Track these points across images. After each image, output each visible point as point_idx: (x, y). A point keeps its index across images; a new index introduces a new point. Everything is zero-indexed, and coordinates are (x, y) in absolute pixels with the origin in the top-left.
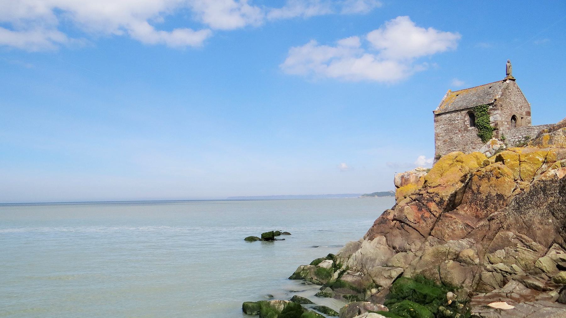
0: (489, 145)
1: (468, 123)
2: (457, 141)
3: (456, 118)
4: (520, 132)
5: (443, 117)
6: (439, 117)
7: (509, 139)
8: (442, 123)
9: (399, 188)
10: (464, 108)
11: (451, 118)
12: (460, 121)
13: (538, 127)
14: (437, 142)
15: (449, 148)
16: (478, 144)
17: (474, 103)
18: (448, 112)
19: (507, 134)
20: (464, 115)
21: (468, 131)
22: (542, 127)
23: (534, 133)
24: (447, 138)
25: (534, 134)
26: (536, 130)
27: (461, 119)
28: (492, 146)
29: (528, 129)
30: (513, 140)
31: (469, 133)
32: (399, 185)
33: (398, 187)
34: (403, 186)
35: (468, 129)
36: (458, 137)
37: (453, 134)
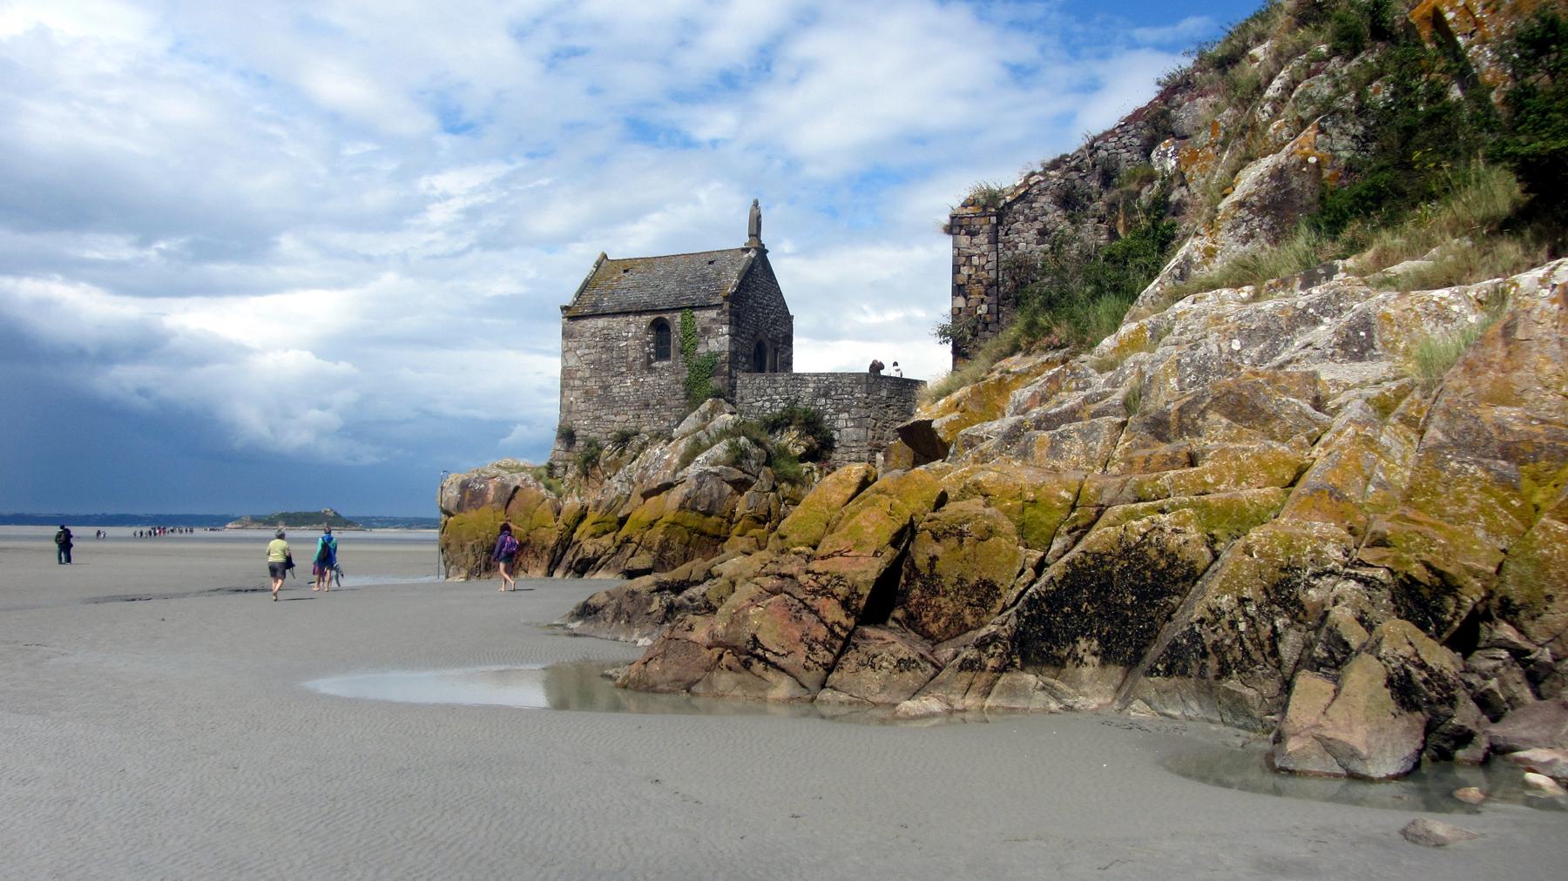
0: (705, 413)
7: (751, 400)
8: (586, 340)
9: (453, 516)
10: (644, 309)
14: (567, 393)
15: (598, 413)
17: (672, 299)
18: (604, 315)
19: (746, 388)
21: (651, 370)
23: (807, 390)
24: (593, 384)
26: (811, 385)
27: (635, 337)
28: (712, 415)
30: (760, 403)
32: (452, 506)
33: (449, 514)
35: (653, 365)
37: (612, 376)
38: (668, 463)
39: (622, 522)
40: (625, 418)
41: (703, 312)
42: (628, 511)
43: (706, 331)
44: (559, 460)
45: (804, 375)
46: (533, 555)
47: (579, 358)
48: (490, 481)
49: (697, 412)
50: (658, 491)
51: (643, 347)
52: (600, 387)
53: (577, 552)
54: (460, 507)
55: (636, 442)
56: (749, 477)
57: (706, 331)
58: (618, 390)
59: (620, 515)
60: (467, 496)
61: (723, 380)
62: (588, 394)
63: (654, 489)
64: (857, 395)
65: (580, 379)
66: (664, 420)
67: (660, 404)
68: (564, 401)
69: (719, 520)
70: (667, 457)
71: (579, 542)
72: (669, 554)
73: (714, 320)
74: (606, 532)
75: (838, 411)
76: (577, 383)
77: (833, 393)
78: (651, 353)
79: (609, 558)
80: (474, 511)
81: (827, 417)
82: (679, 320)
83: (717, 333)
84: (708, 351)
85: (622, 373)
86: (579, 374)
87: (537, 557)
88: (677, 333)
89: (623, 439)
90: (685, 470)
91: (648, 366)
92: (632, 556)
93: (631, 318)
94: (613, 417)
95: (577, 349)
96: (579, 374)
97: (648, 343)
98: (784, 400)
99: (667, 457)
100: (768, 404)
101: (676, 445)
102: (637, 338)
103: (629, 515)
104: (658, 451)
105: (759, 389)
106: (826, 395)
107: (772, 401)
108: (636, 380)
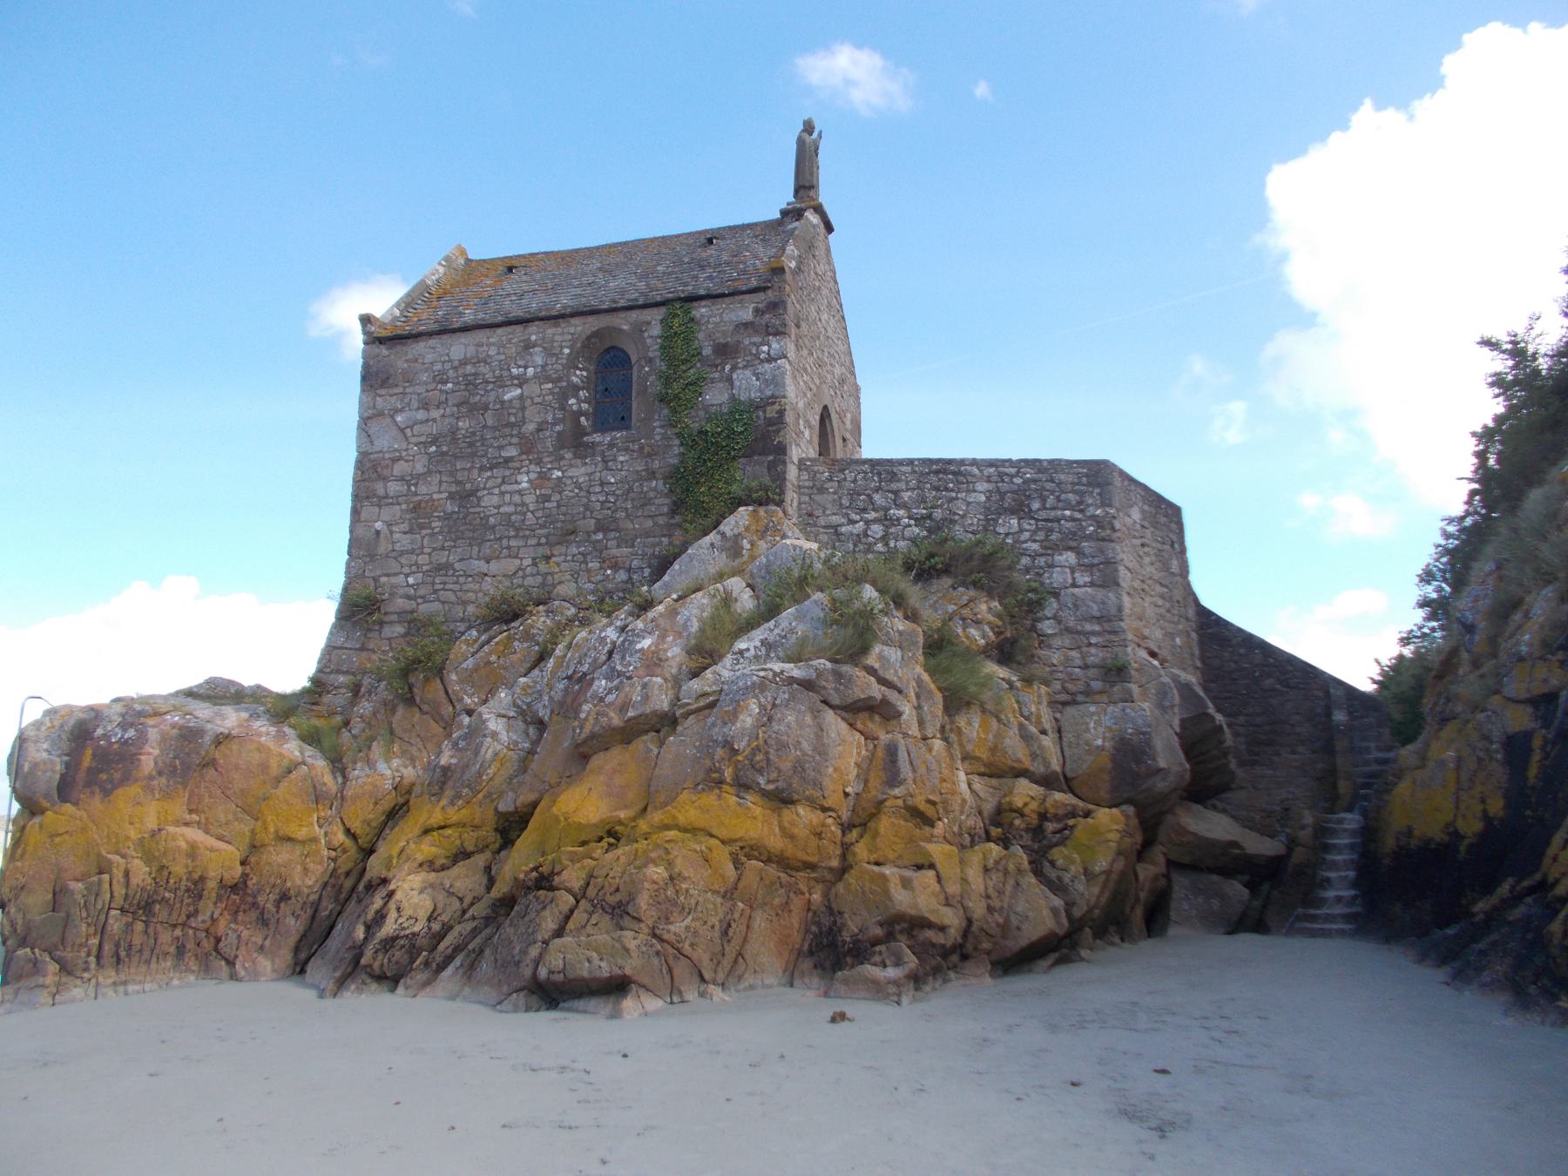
0: (737, 537)
1: (585, 406)
2: (511, 509)
3: (515, 371)
4: (894, 486)
5: (429, 358)
6: (400, 359)
7: (835, 519)
11: (483, 369)
12: (533, 389)
13: (992, 470)
14: (368, 511)
15: (442, 558)
16: (647, 534)
18: (465, 329)
19: (822, 490)
20: (567, 351)
22: (1013, 471)
25: (969, 504)
26: (982, 486)
27: (543, 377)
29: (937, 472)
31: (590, 469)
34: (76, 804)
36: (515, 487)
37: (482, 469)
38: (653, 662)
39: (511, 827)
40: (511, 565)
41: (721, 305)
42: (527, 797)
43: (725, 351)
44: (339, 672)
45: (962, 462)
46: (254, 914)
47: (402, 430)
48: (151, 722)
49: (712, 537)
50: (628, 733)
51: (563, 397)
52: (451, 496)
53: (381, 917)
54: (65, 789)
55: (540, 621)
56: (892, 696)
57: (725, 351)
58: (495, 500)
59: (506, 805)
60: (87, 760)
61: (771, 466)
62: (419, 513)
63: (614, 730)
64: (1091, 511)
65: (402, 479)
66: (615, 567)
67: (601, 527)
68: (360, 531)
69: (815, 817)
70: (646, 643)
71: (385, 881)
72: (678, 927)
73: (746, 325)
74: (462, 855)
75: (1050, 548)
76: (394, 488)
77: (1036, 505)
78: (581, 413)
79: (475, 932)
80: (98, 797)
81: (1025, 561)
82: (656, 330)
83: (757, 356)
84: (733, 398)
85: (508, 460)
86: (400, 468)
87: (263, 921)
88: (650, 361)
89: (506, 614)
90: (708, 674)
91: (575, 442)
92: (559, 933)
93: (534, 333)
94: (481, 566)
95: (397, 411)
96: (400, 468)
97: (577, 388)
98: (919, 521)
99: (646, 643)
100: (877, 530)
101: (673, 613)
102: (548, 379)
103: (535, 805)
104: (611, 634)
105: (854, 494)
106: (1020, 509)
107: (887, 521)
108: (543, 476)
